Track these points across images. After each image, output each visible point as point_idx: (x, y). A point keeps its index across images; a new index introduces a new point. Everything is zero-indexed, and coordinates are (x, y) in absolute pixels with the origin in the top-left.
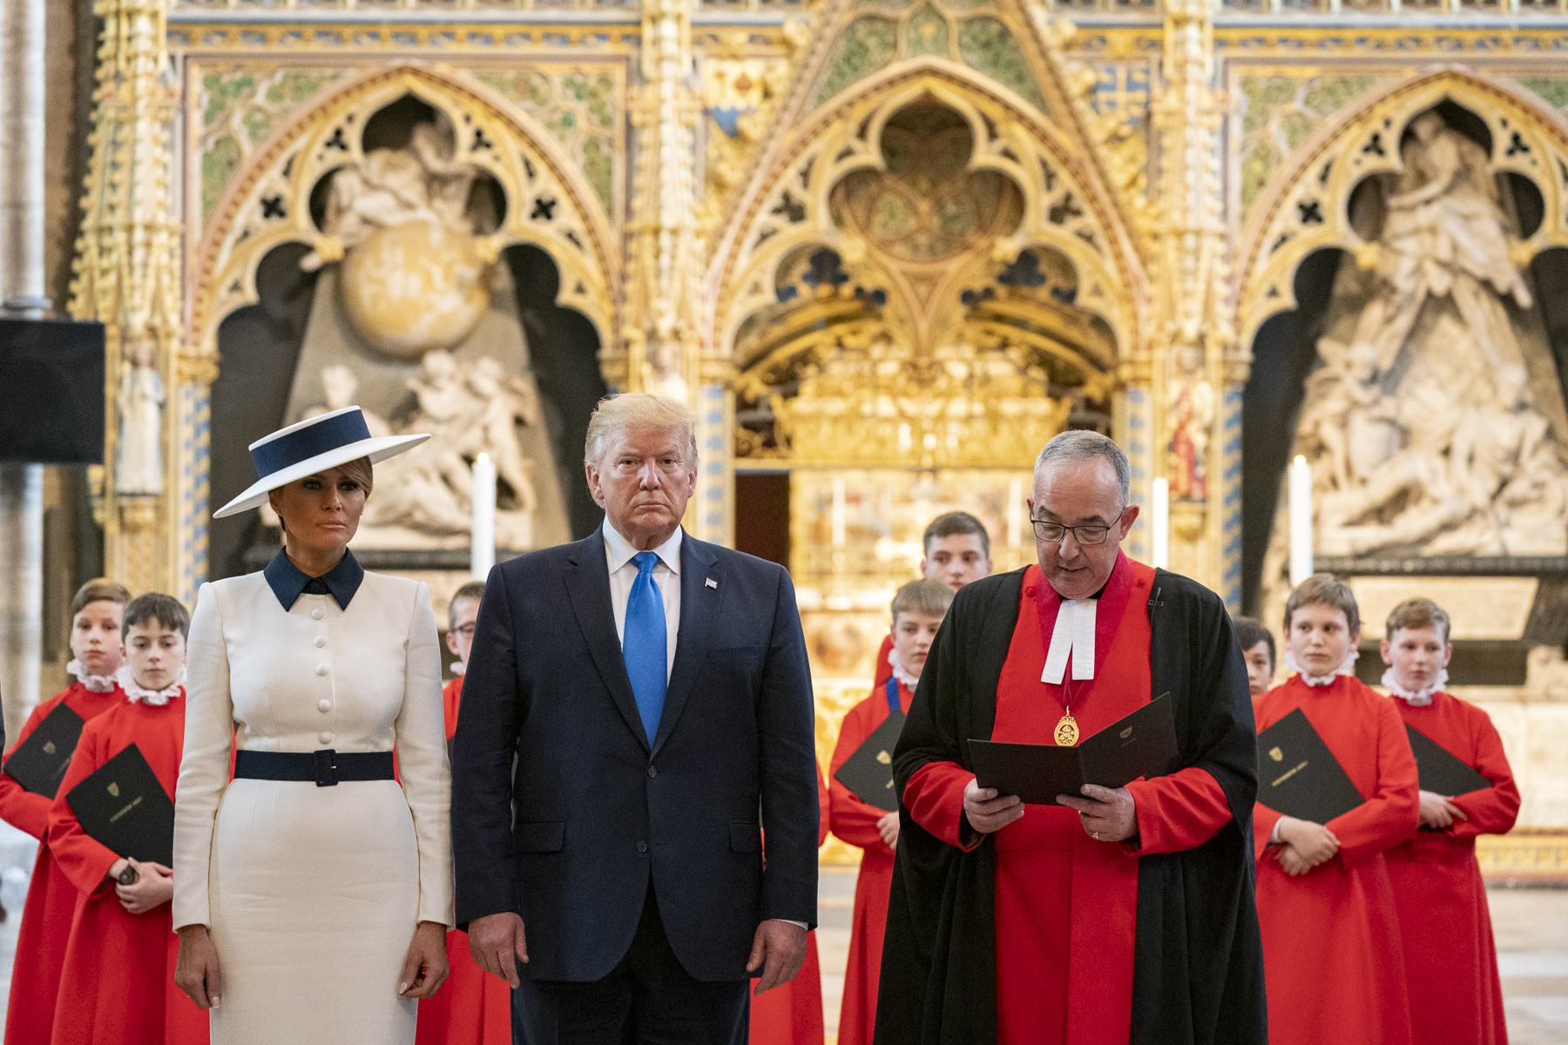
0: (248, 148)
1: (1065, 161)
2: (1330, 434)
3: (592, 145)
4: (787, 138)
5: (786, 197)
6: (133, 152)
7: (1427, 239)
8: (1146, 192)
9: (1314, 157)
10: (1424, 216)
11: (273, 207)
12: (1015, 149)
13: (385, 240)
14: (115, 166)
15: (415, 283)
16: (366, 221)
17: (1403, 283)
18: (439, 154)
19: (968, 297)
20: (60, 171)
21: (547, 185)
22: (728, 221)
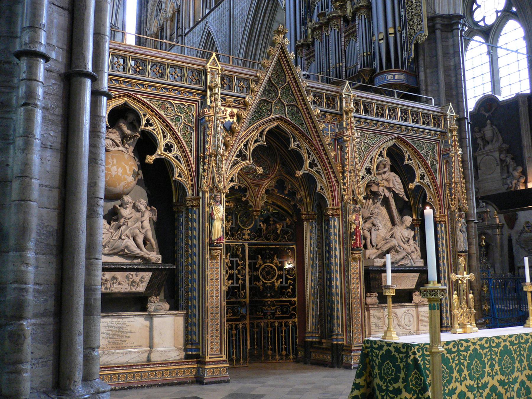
2: (367, 234)
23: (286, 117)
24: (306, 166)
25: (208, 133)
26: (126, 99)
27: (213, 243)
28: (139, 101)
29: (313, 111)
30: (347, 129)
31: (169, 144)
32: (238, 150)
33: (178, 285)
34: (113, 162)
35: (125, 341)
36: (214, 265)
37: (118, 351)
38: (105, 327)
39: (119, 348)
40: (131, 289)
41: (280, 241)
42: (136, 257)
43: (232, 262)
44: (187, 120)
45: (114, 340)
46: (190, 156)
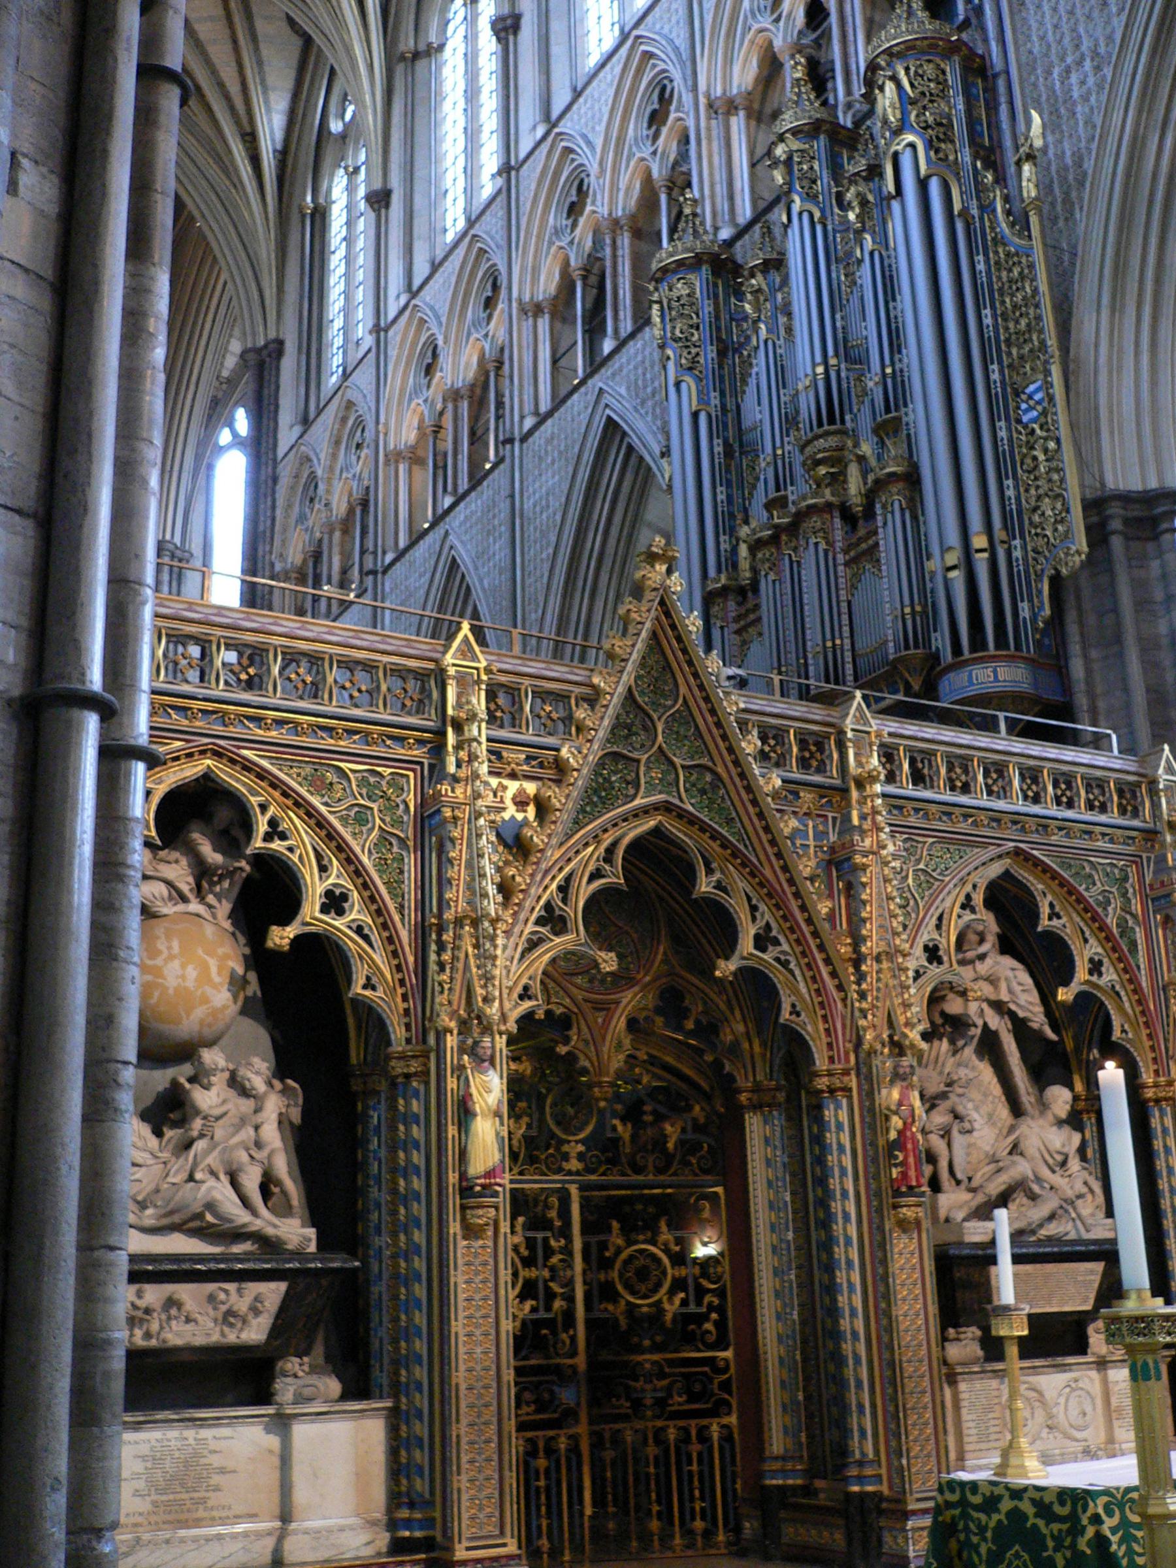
23: (681, 800)
24: (747, 944)
25: (452, 854)
26: (209, 762)
27: (471, 1188)
28: (247, 767)
29: (761, 781)
30: (863, 832)
31: (338, 892)
32: (542, 902)
33: (369, 1320)
34: (170, 948)
35: (204, 1501)
36: (476, 1255)
37: (182, 1533)
38: (143, 1458)
39: (185, 1524)
40: (223, 1334)
41: (675, 1174)
42: (238, 1235)
43: (530, 1243)
44: (388, 819)
45: (171, 1497)
46: (399, 925)
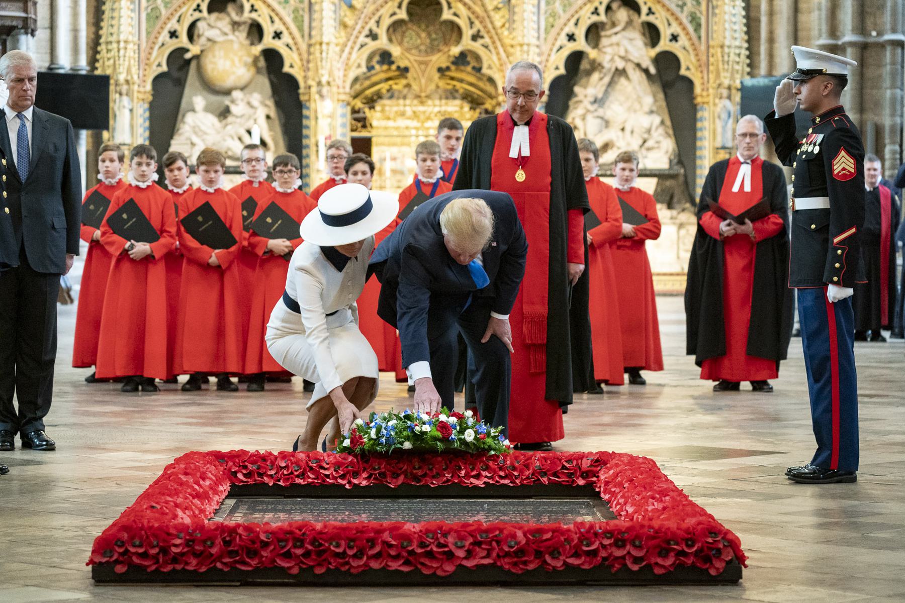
0: (164, 12)
1: (477, 17)
3: (296, 10)
4: (371, 8)
5: (371, 31)
6: (120, 13)
7: (615, 48)
8: (508, 29)
9: (573, 16)
10: (615, 39)
11: (173, 34)
12: (458, 12)
13: (217, 47)
14: (112, 18)
15: (228, 64)
16: (209, 40)
17: (607, 65)
18: (237, 14)
19: (440, 70)
20: (92, 21)
21: (278, 26)
22: (348, 40)
